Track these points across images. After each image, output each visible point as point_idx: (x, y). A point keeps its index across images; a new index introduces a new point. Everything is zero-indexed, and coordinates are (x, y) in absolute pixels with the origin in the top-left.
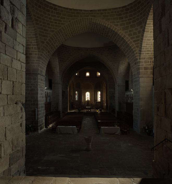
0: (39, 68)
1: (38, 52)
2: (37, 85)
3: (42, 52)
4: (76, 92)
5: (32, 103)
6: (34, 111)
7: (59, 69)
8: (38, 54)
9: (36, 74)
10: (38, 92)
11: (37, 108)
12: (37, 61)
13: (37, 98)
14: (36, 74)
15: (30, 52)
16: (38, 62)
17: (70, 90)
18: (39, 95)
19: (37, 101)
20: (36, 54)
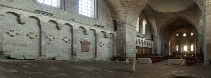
0: (127, 20)
1: (124, 8)
2: (125, 31)
3: (128, 9)
4: (177, 46)
5: (122, 42)
6: (123, 48)
7: (157, 28)
8: (125, 10)
9: (124, 24)
10: (126, 35)
11: (125, 46)
12: (124, 15)
13: (125, 39)
14: (124, 24)
15: (118, 10)
16: (125, 16)
17: (171, 44)
18: (127, 38)
19: (125, 41)
20: (122, 11)
